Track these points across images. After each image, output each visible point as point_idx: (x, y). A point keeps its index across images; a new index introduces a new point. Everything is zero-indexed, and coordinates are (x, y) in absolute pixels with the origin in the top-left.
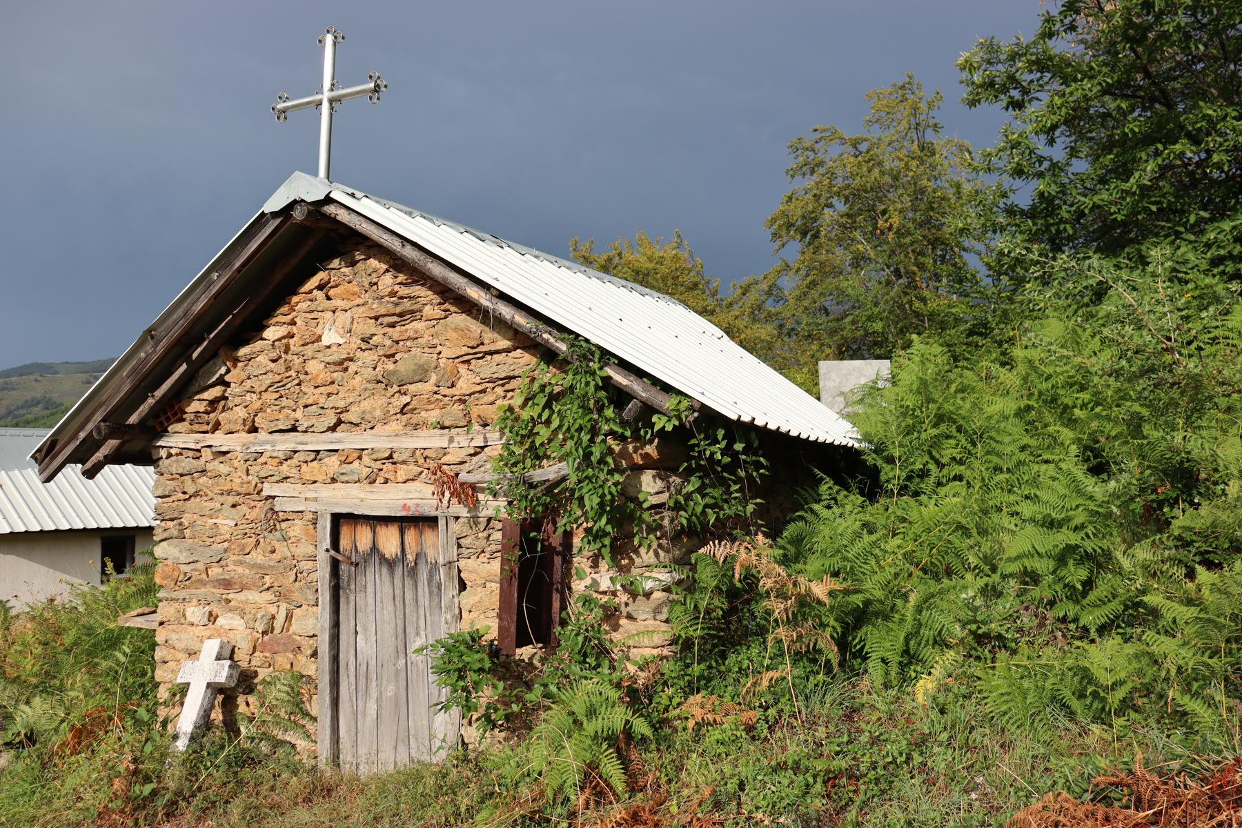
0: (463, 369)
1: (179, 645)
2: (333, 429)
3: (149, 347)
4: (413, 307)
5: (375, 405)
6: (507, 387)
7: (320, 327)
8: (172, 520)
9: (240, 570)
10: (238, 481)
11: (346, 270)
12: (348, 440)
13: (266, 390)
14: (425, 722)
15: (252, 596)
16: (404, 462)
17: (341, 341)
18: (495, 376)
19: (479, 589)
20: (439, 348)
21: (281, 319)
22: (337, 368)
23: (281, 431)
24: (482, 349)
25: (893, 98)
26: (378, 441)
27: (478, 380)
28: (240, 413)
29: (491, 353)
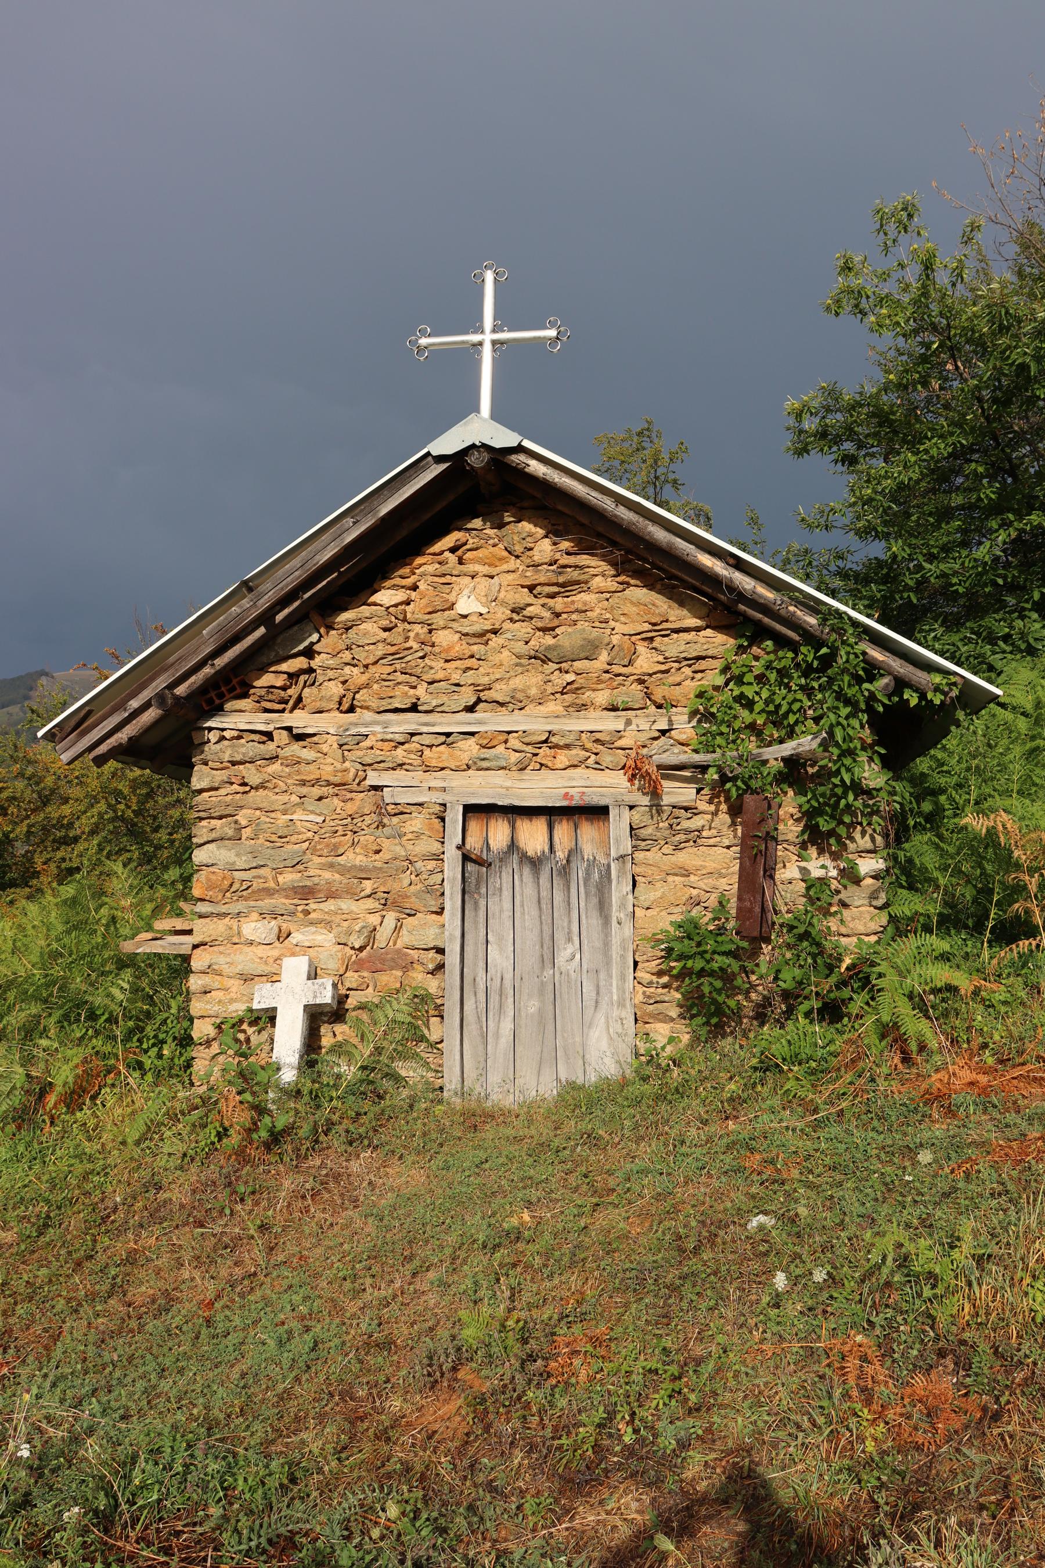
0: (642, 648)
1: (227, 970)
2: (470, 709)
3: (246, 603)
4: (582, 577)
5: (531, 681)
6: (696, 667)
7: (454, 594)
8: (220, 818)
9: (327, 875)
10: (330, 768)
11: (491, 532)
12: (489, 721)
13: (376, 662)
14: (578, 1039)
15: (346, 905)
16: (567, 746)
17: (484, 610)
18: (683, 655)
19: (658, 885)
20: (612, 624)
21: (398, 581)
22: (478, 640)
23: (396, 710)
24: (665, 625)
25: (626, 445)
26: (533, 722)
27: (661, 658)
28: (335, 689)
29: (677, 631)
